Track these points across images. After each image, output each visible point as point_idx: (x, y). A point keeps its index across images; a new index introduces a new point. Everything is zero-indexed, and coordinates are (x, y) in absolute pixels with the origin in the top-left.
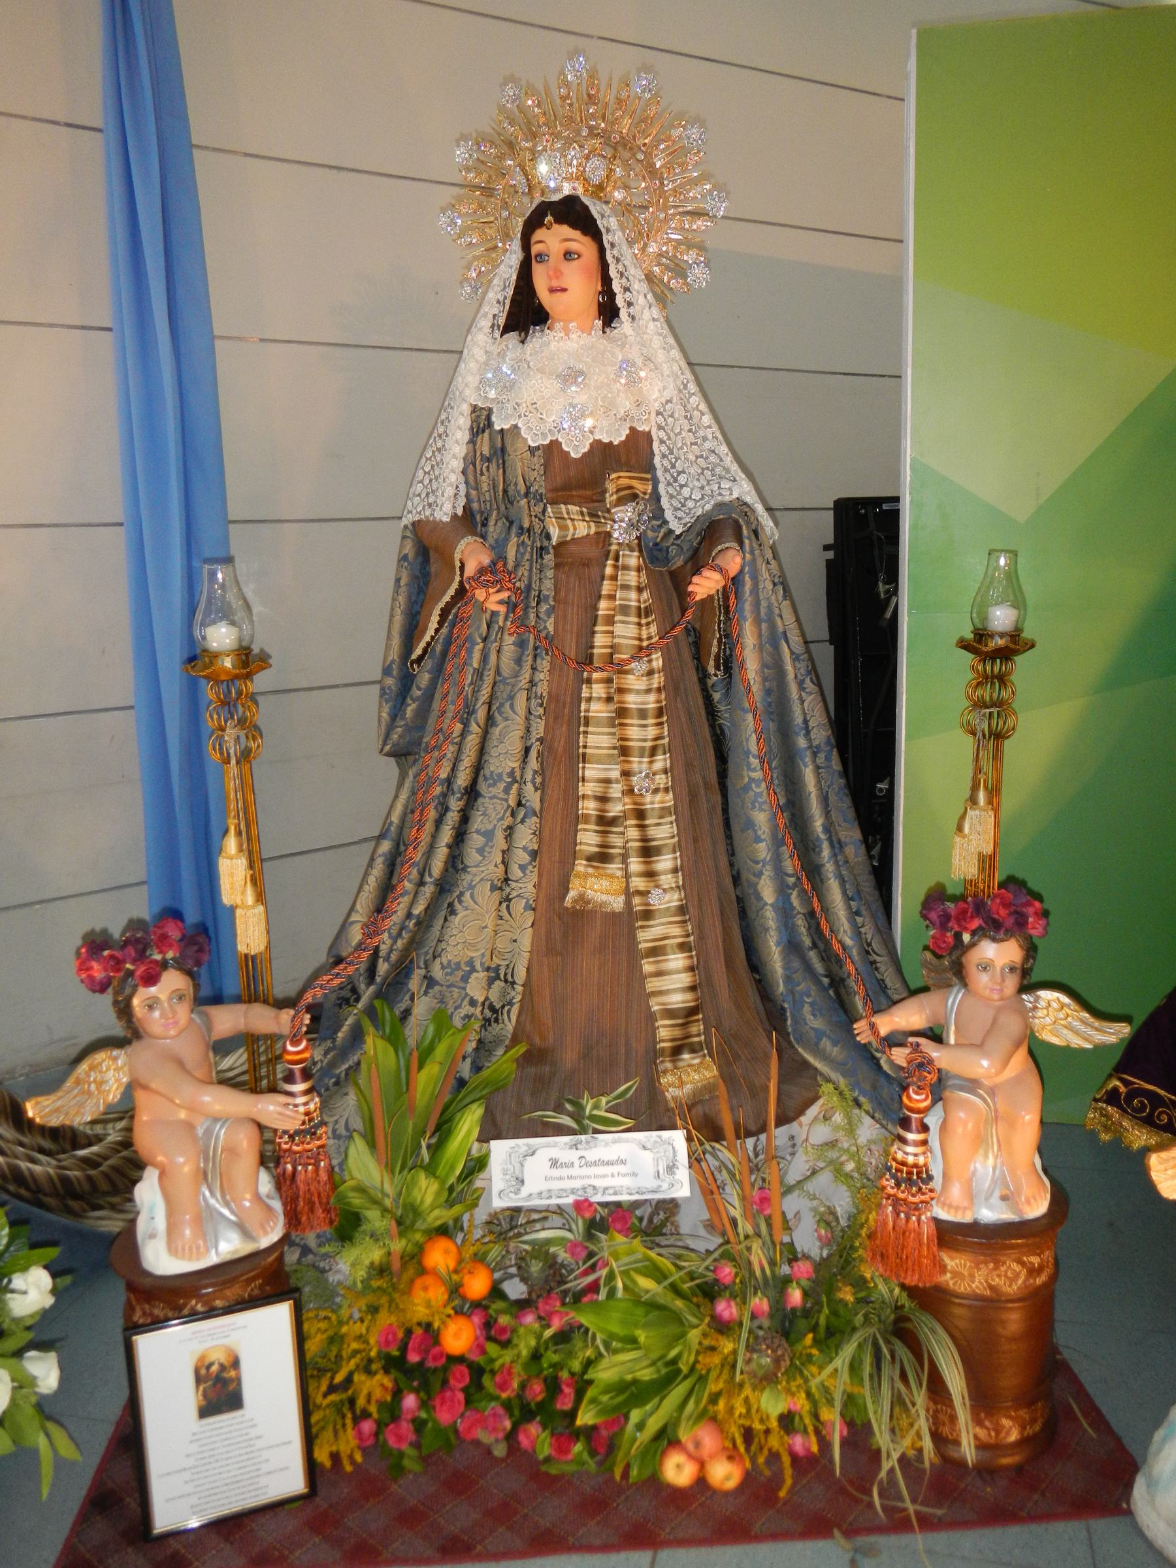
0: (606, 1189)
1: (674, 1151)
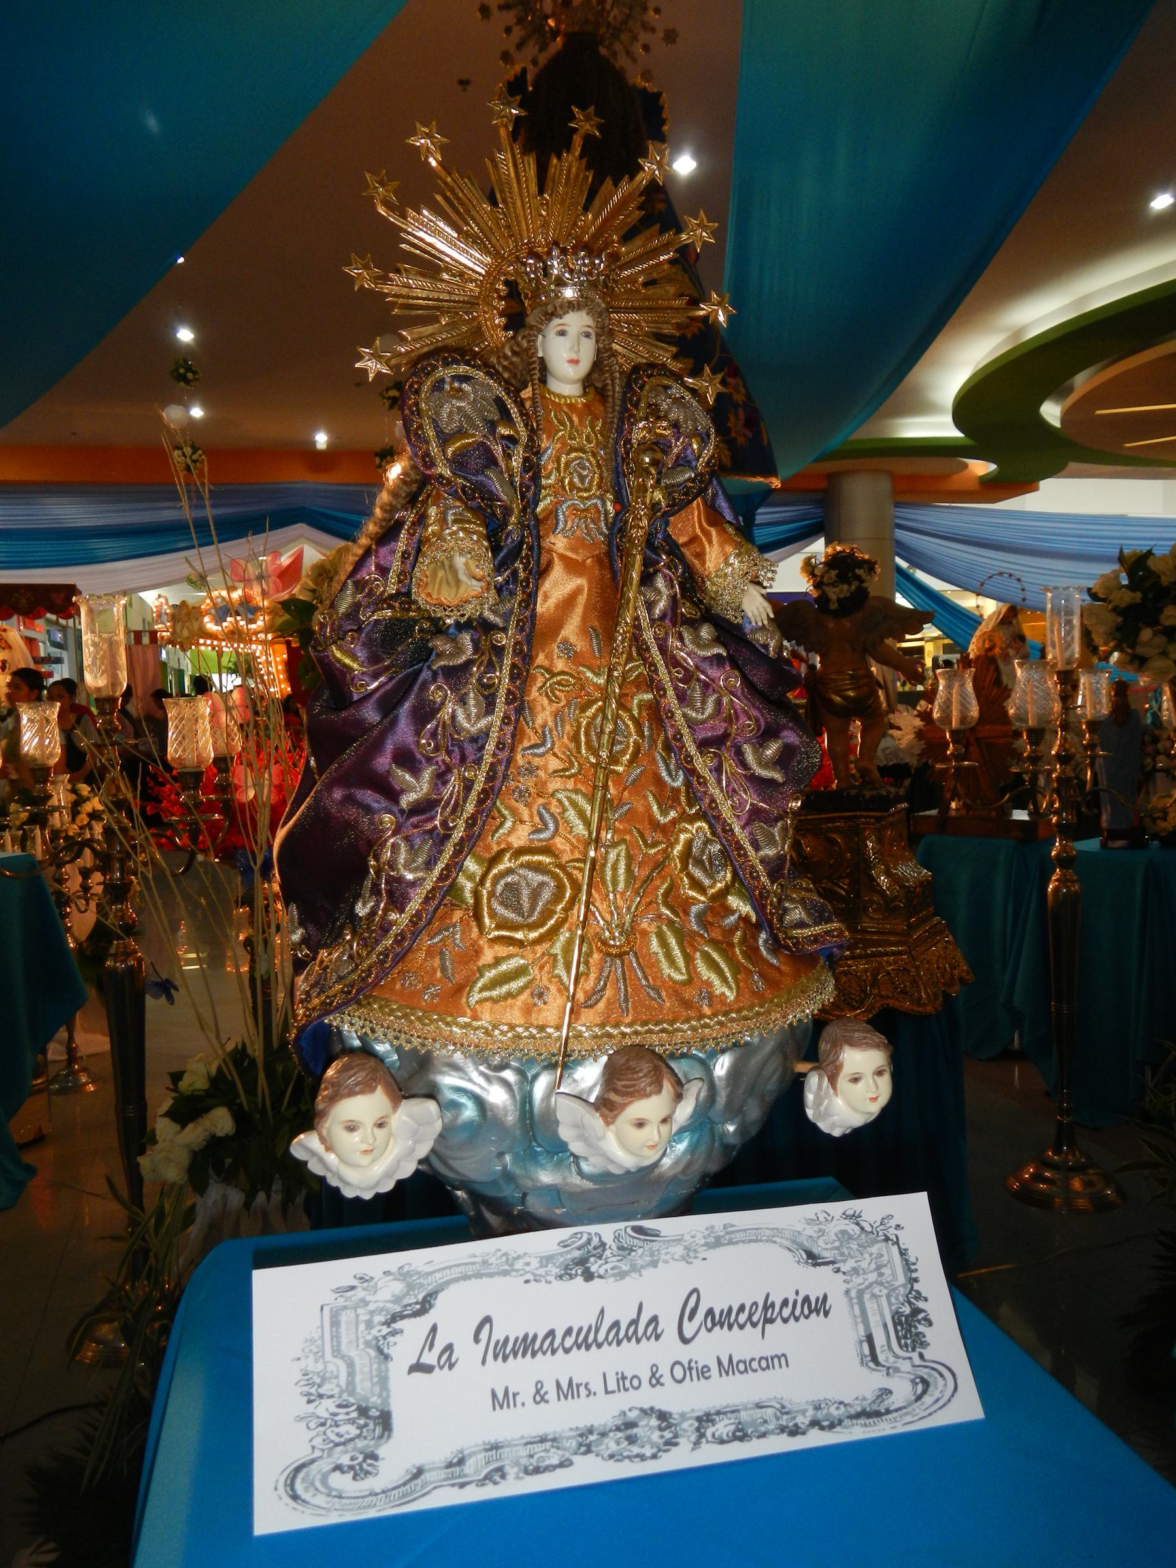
0: (705, 1419)
1: (909, 1266)
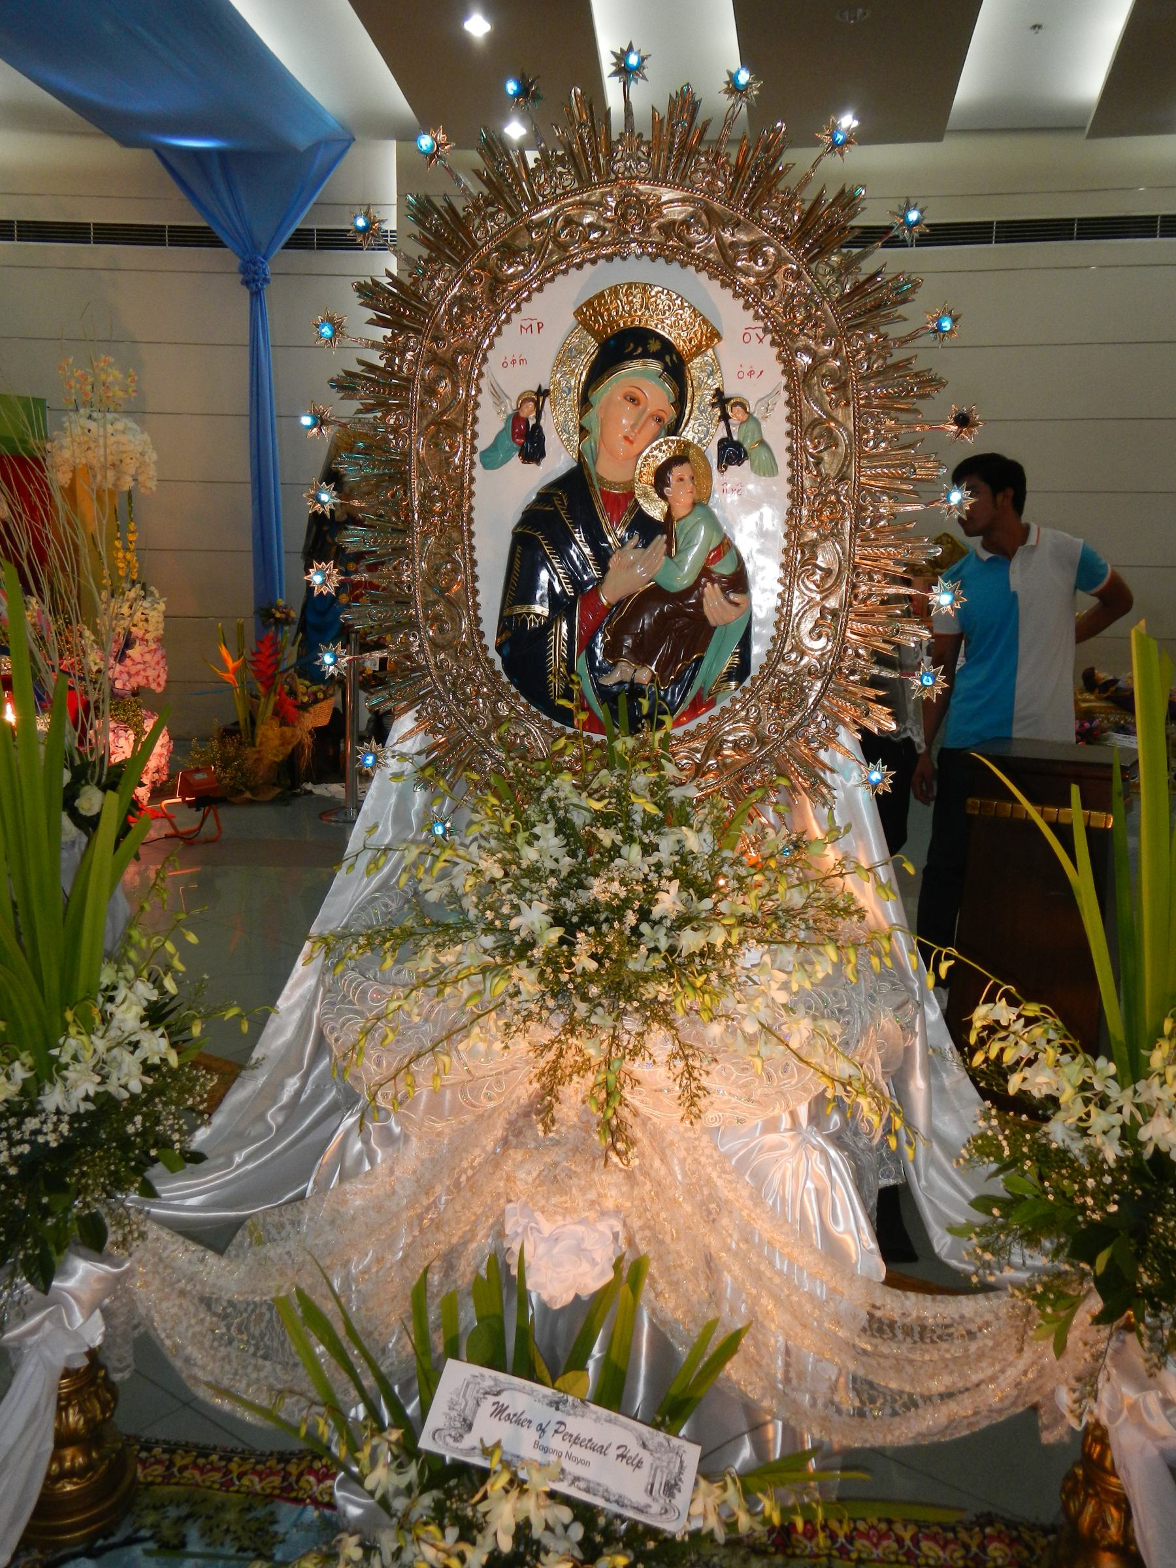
1: (681, 1467)
